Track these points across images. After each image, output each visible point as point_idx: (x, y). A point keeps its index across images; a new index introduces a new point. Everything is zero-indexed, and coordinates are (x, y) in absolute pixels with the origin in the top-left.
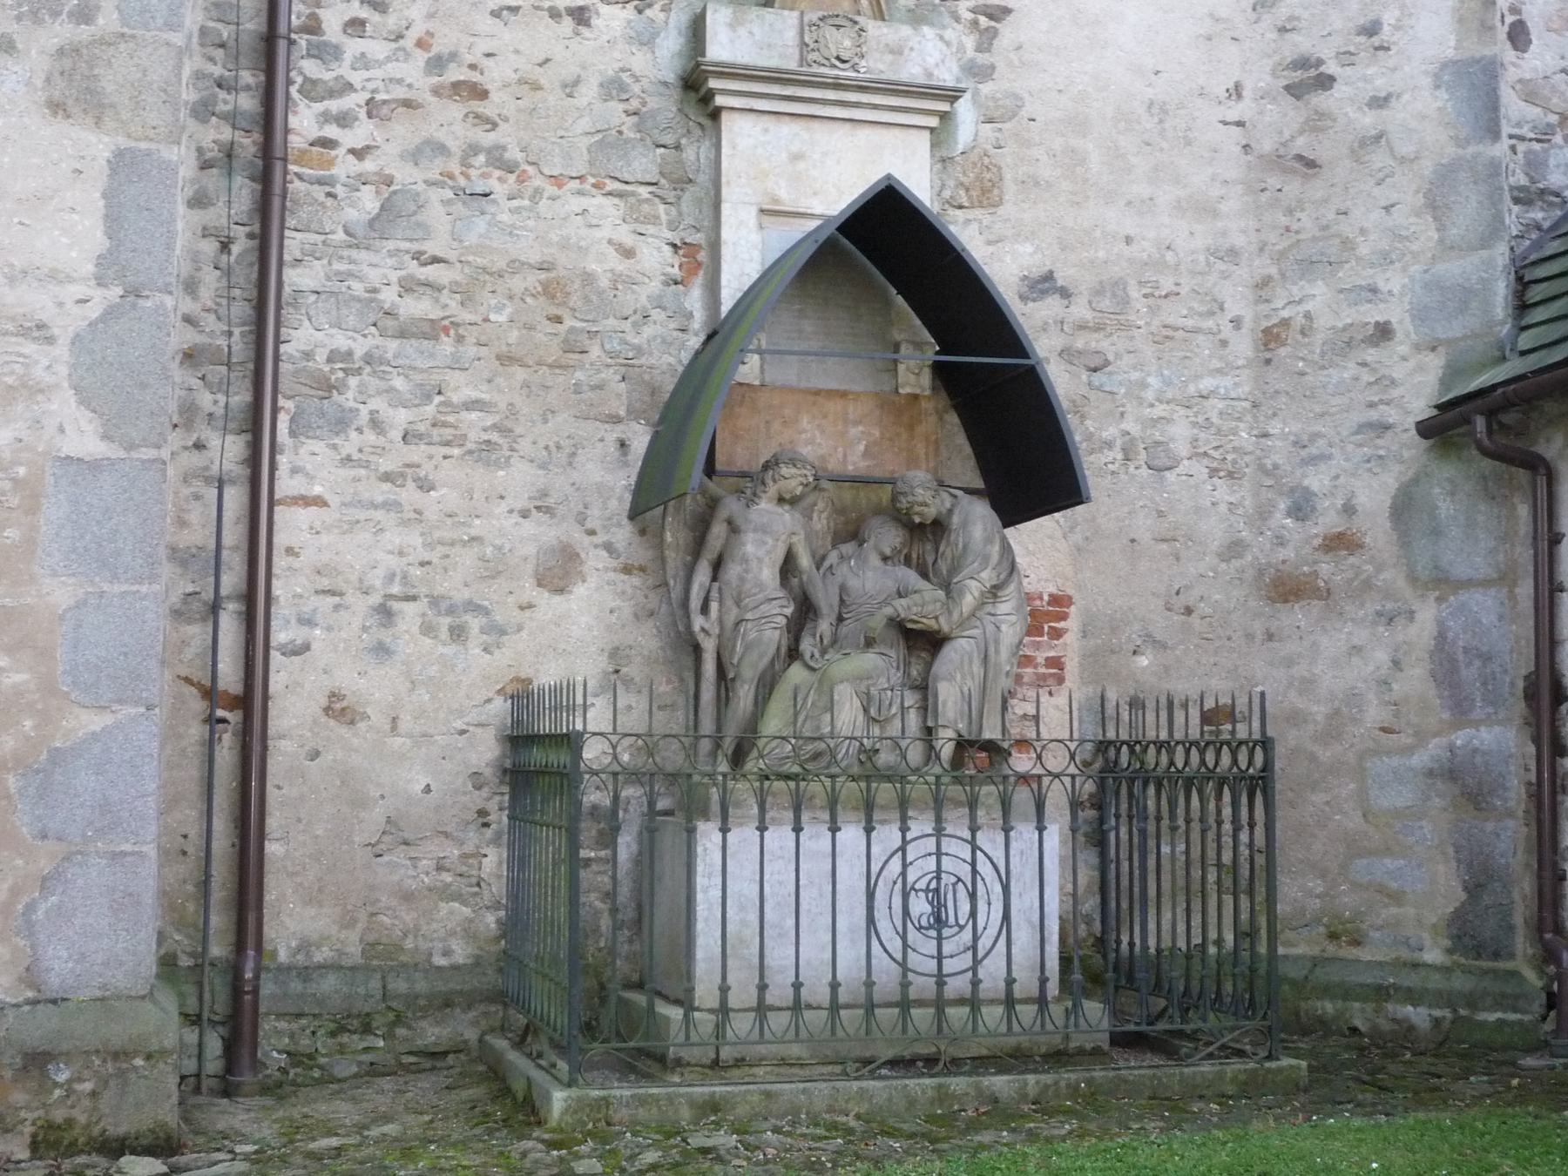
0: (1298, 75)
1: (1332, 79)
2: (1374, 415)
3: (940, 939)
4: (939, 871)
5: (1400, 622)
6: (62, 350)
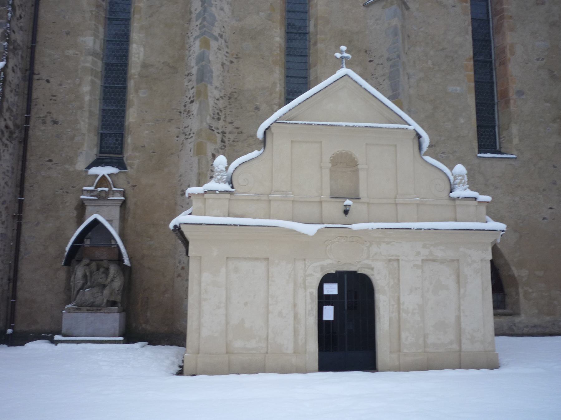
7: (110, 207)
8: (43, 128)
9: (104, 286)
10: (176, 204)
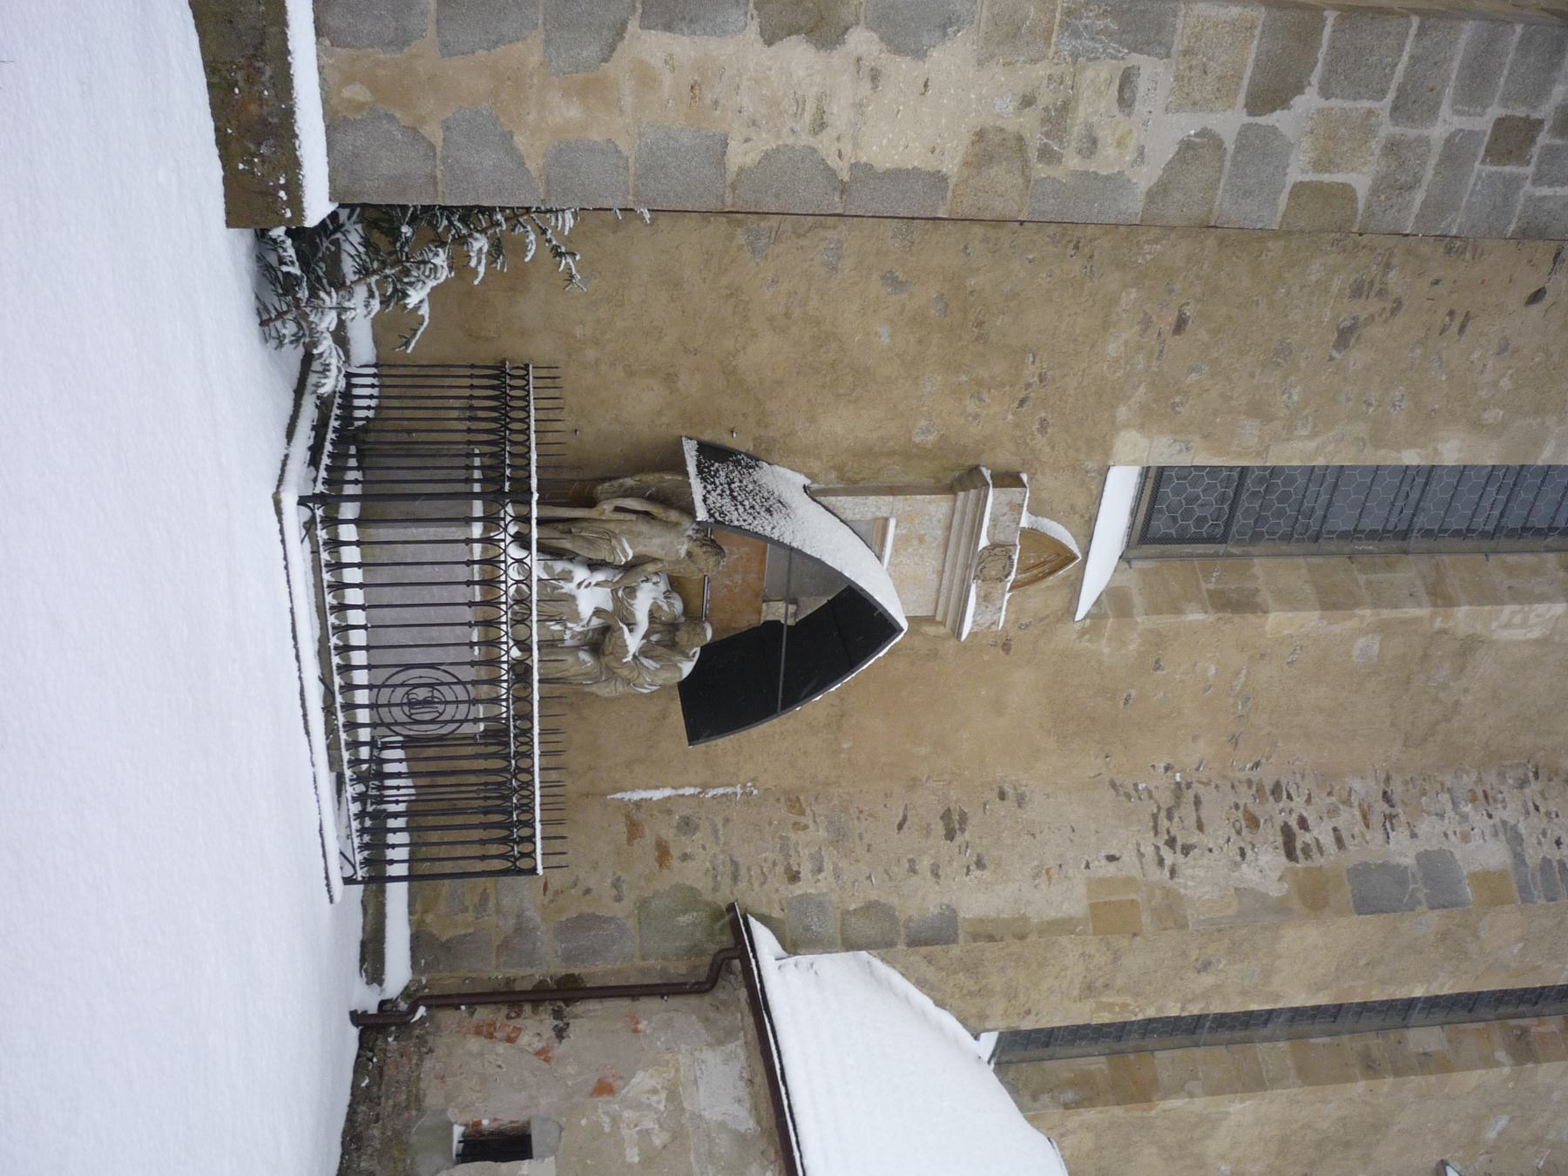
0: (956, 817)
1: (952, 839)
2: (743, 871)
3: (401, 705)
4: (447, 703)
5: (614, 892)
6: (805, 140)
7: (935, 584)
8: (1336, 285)
10: (913, 784)
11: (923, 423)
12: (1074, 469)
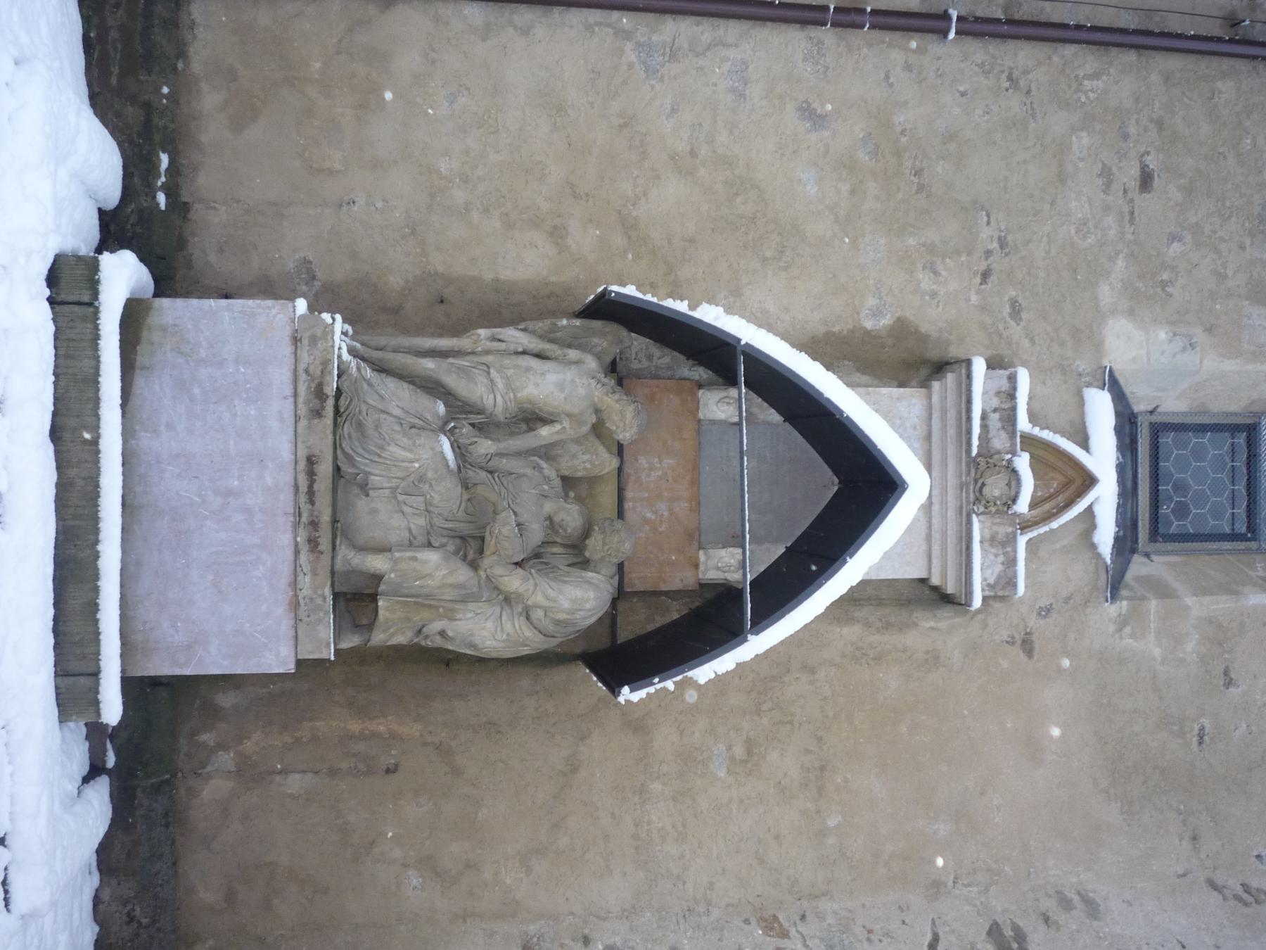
0: (1009, 933)
9: (470, 544)
11: (872, 302)
12: (1064, 372)
